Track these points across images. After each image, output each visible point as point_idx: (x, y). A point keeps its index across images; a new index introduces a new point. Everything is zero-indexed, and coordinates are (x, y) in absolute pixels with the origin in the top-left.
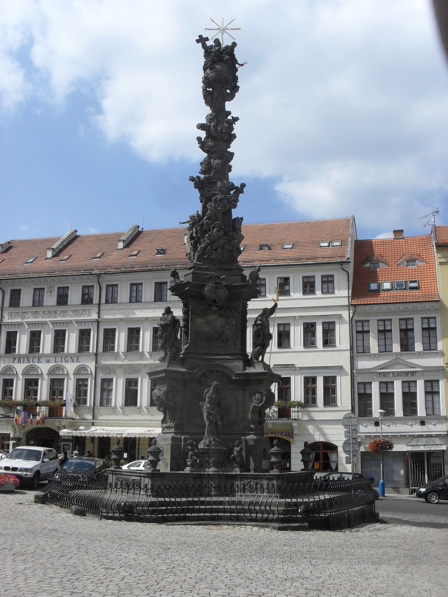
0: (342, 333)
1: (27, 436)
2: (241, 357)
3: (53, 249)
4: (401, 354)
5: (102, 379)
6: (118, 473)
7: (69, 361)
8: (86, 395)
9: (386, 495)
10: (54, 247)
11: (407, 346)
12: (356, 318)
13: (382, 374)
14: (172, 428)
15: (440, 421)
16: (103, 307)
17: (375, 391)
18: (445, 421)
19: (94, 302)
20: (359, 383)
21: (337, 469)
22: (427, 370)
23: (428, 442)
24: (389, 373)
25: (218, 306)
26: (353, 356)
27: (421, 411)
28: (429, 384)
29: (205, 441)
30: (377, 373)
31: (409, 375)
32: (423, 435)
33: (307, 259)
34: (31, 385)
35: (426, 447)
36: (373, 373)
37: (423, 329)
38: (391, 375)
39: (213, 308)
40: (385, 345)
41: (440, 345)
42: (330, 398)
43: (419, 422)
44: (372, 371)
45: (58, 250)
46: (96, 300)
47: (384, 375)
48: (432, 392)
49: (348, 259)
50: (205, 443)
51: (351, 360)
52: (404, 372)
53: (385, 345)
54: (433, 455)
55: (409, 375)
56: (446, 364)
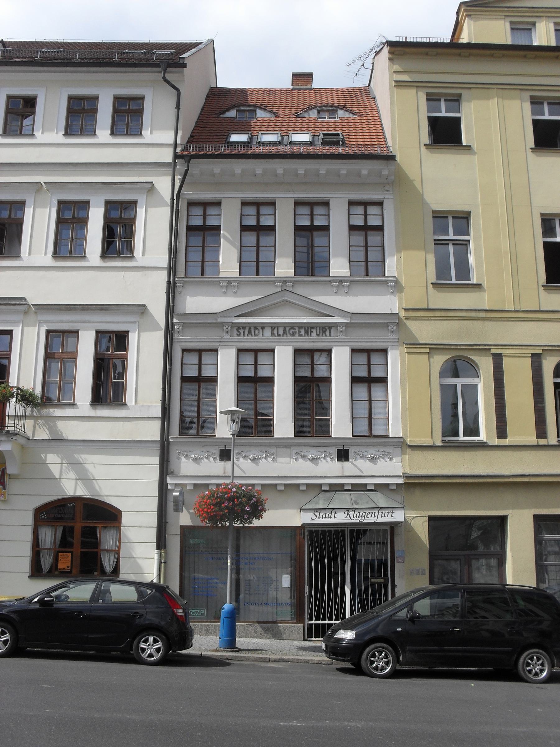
0: (153, 229)
4: (295, 282)
9: (240, 642)
11: (311, 263)
12: (190, 194)
13: (244, 328)
15: (387, 449)
17: (225, 368)
18: (399, 450)
20: (184, 351)
21: (116, 570)
22: (359, 322)
23: (357, 503)
24: (263, 326)
26: (175, 283)
27: (340, 425)
28: (362, 359)
30: (233, 325)
31: (314, 334)
32: (343, 485)
35: (351, 514)
36: (222, 324)
37: (352, 228)
38: (268, 332)
40: (258, 261)
41: (392, 266)
42: (108, 386)
43: (334, 451)
44: (220, 320)
47: (250, 332)
48: (368, 380)
51: (168, 293)
52: (300, 326)
53: (258, 261)
54: (367, 538)
55: (314, 334)
56: (406, 310)
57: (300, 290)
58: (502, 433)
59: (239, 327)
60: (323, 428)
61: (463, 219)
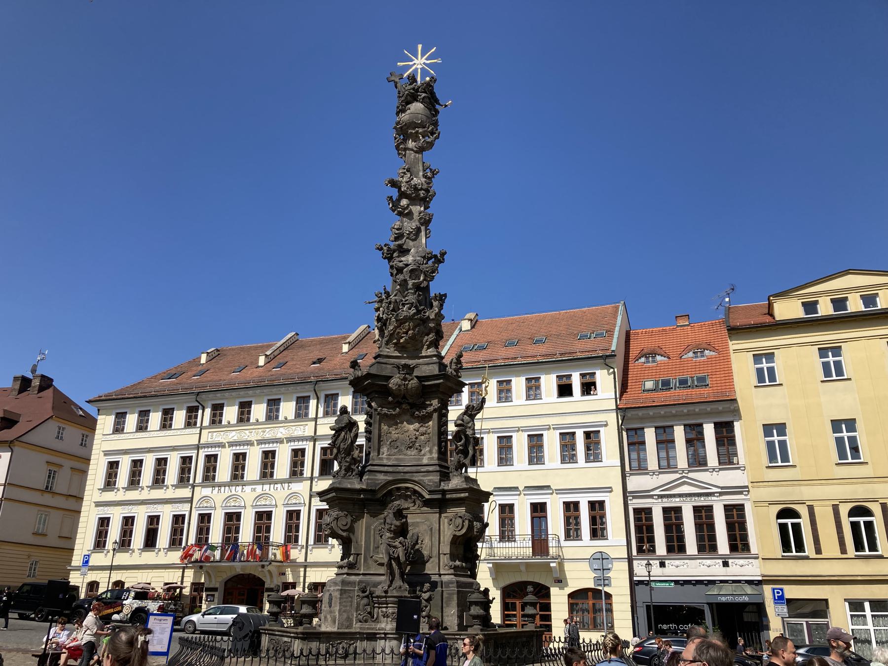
1: (225, 585)
2: (438, 468)
3: (266, 356)
8: (297, 531)
10: (268, 353)
16: (319, 421)
22: (726, 491)
25: (409, 404)
30: (658, 495)
33: (561, 354)
34: (233, 519)
39: (404, 406)
43: (720, 561)
44: (651, 493)
45: (272, 356)
46: (312, 414)
49: (613, 351)
54: (747, 610)
57: (691, 475)
58: (818, 551)
59: (661, 496)
60: (713, 548)
61: (781, 428)
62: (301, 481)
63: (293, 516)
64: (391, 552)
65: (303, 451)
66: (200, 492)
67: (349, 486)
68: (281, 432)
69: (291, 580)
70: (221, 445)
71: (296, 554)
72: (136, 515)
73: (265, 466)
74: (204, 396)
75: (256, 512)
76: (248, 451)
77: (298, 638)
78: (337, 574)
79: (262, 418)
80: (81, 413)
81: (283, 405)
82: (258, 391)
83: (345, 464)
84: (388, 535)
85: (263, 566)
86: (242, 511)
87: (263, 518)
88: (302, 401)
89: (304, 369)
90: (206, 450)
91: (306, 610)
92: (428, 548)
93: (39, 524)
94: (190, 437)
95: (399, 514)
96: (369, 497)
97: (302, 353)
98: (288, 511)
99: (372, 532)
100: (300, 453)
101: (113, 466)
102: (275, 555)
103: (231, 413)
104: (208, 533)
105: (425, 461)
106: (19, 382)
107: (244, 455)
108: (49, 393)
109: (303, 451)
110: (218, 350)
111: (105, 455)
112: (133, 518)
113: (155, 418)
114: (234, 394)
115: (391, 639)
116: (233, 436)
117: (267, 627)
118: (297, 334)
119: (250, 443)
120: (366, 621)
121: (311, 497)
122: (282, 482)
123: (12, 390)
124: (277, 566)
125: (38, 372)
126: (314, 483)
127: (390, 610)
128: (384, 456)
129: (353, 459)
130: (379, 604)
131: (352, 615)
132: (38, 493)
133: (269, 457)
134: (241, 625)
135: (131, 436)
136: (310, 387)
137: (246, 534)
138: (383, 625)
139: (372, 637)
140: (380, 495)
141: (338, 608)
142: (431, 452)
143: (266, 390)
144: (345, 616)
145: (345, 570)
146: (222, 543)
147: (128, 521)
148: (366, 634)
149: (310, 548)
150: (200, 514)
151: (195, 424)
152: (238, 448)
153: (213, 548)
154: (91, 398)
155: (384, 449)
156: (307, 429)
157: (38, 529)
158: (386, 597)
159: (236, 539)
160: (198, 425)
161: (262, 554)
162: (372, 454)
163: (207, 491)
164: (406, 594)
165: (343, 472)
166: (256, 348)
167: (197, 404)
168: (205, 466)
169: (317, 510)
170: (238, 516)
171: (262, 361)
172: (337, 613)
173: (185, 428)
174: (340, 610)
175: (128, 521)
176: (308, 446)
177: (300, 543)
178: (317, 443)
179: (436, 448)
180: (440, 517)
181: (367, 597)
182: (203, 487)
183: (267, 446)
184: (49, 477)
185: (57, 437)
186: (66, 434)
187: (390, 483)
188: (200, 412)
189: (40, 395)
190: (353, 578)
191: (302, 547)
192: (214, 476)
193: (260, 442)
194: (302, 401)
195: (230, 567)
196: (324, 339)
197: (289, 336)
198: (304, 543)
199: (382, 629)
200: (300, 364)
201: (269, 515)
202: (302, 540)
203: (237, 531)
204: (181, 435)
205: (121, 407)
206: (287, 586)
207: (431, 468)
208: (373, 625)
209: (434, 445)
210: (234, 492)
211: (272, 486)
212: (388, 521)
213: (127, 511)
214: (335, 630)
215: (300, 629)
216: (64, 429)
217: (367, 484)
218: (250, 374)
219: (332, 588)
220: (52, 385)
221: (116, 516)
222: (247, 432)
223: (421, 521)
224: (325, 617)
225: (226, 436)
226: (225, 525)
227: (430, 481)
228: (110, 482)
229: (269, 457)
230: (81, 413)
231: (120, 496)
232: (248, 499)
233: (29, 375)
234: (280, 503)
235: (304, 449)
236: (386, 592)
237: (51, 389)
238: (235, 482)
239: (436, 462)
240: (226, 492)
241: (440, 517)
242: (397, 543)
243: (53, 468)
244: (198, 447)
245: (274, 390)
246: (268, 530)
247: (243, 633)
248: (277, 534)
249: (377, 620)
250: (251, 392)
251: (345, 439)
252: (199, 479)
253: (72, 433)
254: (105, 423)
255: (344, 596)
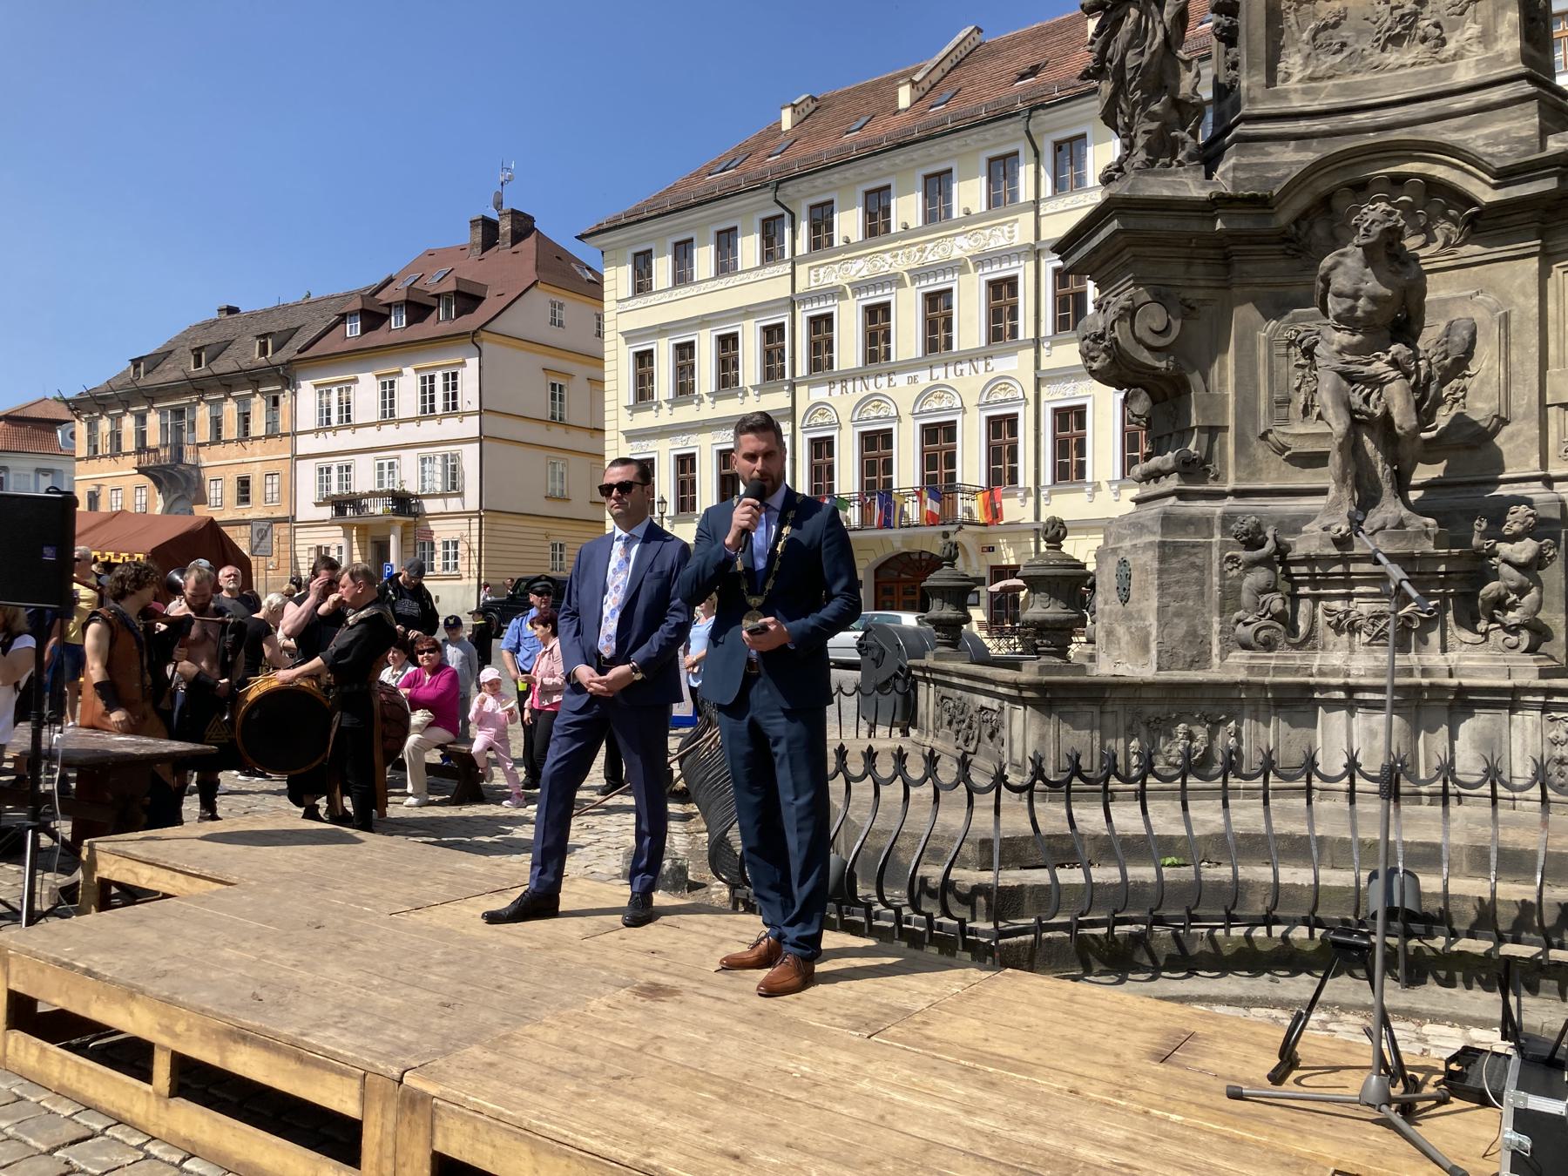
2: (1527, 88)
5: (1056, 411)
6: (939, 677)
7: (966, 373)
8: (1014, 459)
10: (917, 78)
14: (1167, 474)
16: (1045, 209)
19: (1022, 199)
29: (1326, 522)
34: (876, 444)
45: (927, 86)
46: (1026, 192)
50: (1325, 529)
62: (1013, 352)
63: (1001, 428)
64: (1357, 400)
65: (1011, 283)
66: (807, 397)
67: (1166, 193)
68: (960, 246)
69: (1013, 562)
70: (837, 293)
71: (1016, 509)
72: (696, 450)
73: (931, 326)
74: (789, 189)
75: (923, 426)
76: (892, 299)
77: (1025, 702)
78: (1138, 501)
79: (916, 221)
80: (590, 276)
81: (956, 188)
82: (899, 157)
83: (1144, 126)
84: (1343, 338)
85: (946, 535)
86: (894, 426)
87: (939, 437)
88: (1001, 170)
89: (1005, 94)
90: (808, 307)
91: (1038, 608)
92: (1492, 389)
93: (554, 480)
94: (773, 285)
95: (1388, 253)
96: (1245, 224)
97: (991, 66)
98: (989, 419)
99: (1262, 351)
100: (1005, 288)
101: (644, 359)
102: (970, 511)
103: (848, 223)
104: (831, 478)
105: (1464, 74)
106: (480, 230)
107: (885, 308)
108: (529, 243)
109: (1011, 283)
110: (814, 99)
111: (628, 340)
112: (692, 457)
113: (704, 258)
114: (850, 172)
115: (1368, 705)
116: (860, 269)
117: (929, 661)
118: (979, 30)
119: (894, 281)
120: (1269, 645)
121: (1038, 383)
122: (971, 357)
123: (473, 245)
124: (975, 534)
125: (506, 207)
126: (1044, 352)
127: (1364, 608)
128: (1292, 84)
129: (1178, 104)
130: (1313, 582)
131: (1208, 625)
132: (541, 427)
133: (937, 307)
134: (876, 652)
135: (666, 297)
136: (1014, 128)
137: (907, 470)
138: (1336, 659)
139: (1298, 702)
140: (1283, 218)
141: (1154, 603)
142: (1486, 38)
143: (917, 152)
144: (1181, 627)
145: (1172, 483)
146: (861, 494)
147: (686, 463)
148: (1275, 687)
149: (1044, 492)
150: (812, 441)
151: (782, 249)
152: (871, 294)
153: (845, 503)
154: (586, 230)
155: (1293, 63)
156: (1020, 231)
157: (554, 490)
158: (1345, 560)
159: (889, 483)
160: (787, 255)
161: (942, 509)
162: (1244, 84)
163: (820, 393)
164: (1429, 547)
165: (1141, 156)
166: (894, 79)
167: (779, 211)
168: (810, 341)
169: (1056, 411)
170: (887, 436)
171: (904, 97)
172: (1152, 621)
173: (763, 265)
174: (1161, 610)
175: (686, 463)
176: (1024, 272)
177: (1021, 484)
178: (1043, 261)
179: (1513, 15)
180: (1544, 274)
181: (1266, 562)
182: (812, 384)
183: (932, 281)
184: (553, 397)
185: (553, 322)
186: (564, 315)
187: (1316, 167)
188: (787, 232)
189: (515, 248)
190: (1199, 507)
191: (1027, 491)
192: (831, 359)
193: (918, 274)
194: (1001, 170)
195: (882, 540)
196: (1039, 29)
197: (962, 35)
198: (1031, 484)
199: (1335, 672)
200: (989, 87)
201: (949, 429)
202: (1025, 477)
203: (888, 466)
204: (759, 283)
205: (638, 237)
206: (1000, 572)
207: (1496, 95)
208: (1297, 658)
209: (1500, 9)
210: (873, 390)
211: (951, 369)
212: (1340, 282)
213: (682, 445)
214: (1144, 670)
215: (1029, 673)
216: (561, 306)
217: (1235, 183)
218: (883, 128)
219: (1127, 544)
220: (533, 229)
221: (664, 455)
222: (887, 256)
223: (1470, 290)
224: (1110, 633)
225: (843, 272)
226: (862, 458)
227: (1494, 139)
228: (643, 393)
229: (937, 307)
230: (590, 276)
231: (665, 417)
232: (903, 401)
233: (493, 215)
234: (971, 402)
235: (1015, 278)
236: (1342, 542)
237: (533, 236)
238: (873, 367)
239: (1520, 68)
240: (857, 390)
241: (1544, 274)
242: (1380, 367)
243: (559, 381)
244: (792, 303)
245: (935, 148)
246: (951, 461)
247: (883, 674)
248: (971, 466)
249: (1309, 641)
250: (883, 163)
251: (1139, 34)
252: (802, 369)
253: (574, 308)
254: (618, 279)
255: (1175, 564)
